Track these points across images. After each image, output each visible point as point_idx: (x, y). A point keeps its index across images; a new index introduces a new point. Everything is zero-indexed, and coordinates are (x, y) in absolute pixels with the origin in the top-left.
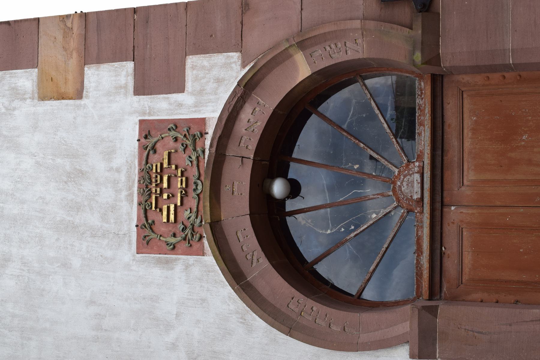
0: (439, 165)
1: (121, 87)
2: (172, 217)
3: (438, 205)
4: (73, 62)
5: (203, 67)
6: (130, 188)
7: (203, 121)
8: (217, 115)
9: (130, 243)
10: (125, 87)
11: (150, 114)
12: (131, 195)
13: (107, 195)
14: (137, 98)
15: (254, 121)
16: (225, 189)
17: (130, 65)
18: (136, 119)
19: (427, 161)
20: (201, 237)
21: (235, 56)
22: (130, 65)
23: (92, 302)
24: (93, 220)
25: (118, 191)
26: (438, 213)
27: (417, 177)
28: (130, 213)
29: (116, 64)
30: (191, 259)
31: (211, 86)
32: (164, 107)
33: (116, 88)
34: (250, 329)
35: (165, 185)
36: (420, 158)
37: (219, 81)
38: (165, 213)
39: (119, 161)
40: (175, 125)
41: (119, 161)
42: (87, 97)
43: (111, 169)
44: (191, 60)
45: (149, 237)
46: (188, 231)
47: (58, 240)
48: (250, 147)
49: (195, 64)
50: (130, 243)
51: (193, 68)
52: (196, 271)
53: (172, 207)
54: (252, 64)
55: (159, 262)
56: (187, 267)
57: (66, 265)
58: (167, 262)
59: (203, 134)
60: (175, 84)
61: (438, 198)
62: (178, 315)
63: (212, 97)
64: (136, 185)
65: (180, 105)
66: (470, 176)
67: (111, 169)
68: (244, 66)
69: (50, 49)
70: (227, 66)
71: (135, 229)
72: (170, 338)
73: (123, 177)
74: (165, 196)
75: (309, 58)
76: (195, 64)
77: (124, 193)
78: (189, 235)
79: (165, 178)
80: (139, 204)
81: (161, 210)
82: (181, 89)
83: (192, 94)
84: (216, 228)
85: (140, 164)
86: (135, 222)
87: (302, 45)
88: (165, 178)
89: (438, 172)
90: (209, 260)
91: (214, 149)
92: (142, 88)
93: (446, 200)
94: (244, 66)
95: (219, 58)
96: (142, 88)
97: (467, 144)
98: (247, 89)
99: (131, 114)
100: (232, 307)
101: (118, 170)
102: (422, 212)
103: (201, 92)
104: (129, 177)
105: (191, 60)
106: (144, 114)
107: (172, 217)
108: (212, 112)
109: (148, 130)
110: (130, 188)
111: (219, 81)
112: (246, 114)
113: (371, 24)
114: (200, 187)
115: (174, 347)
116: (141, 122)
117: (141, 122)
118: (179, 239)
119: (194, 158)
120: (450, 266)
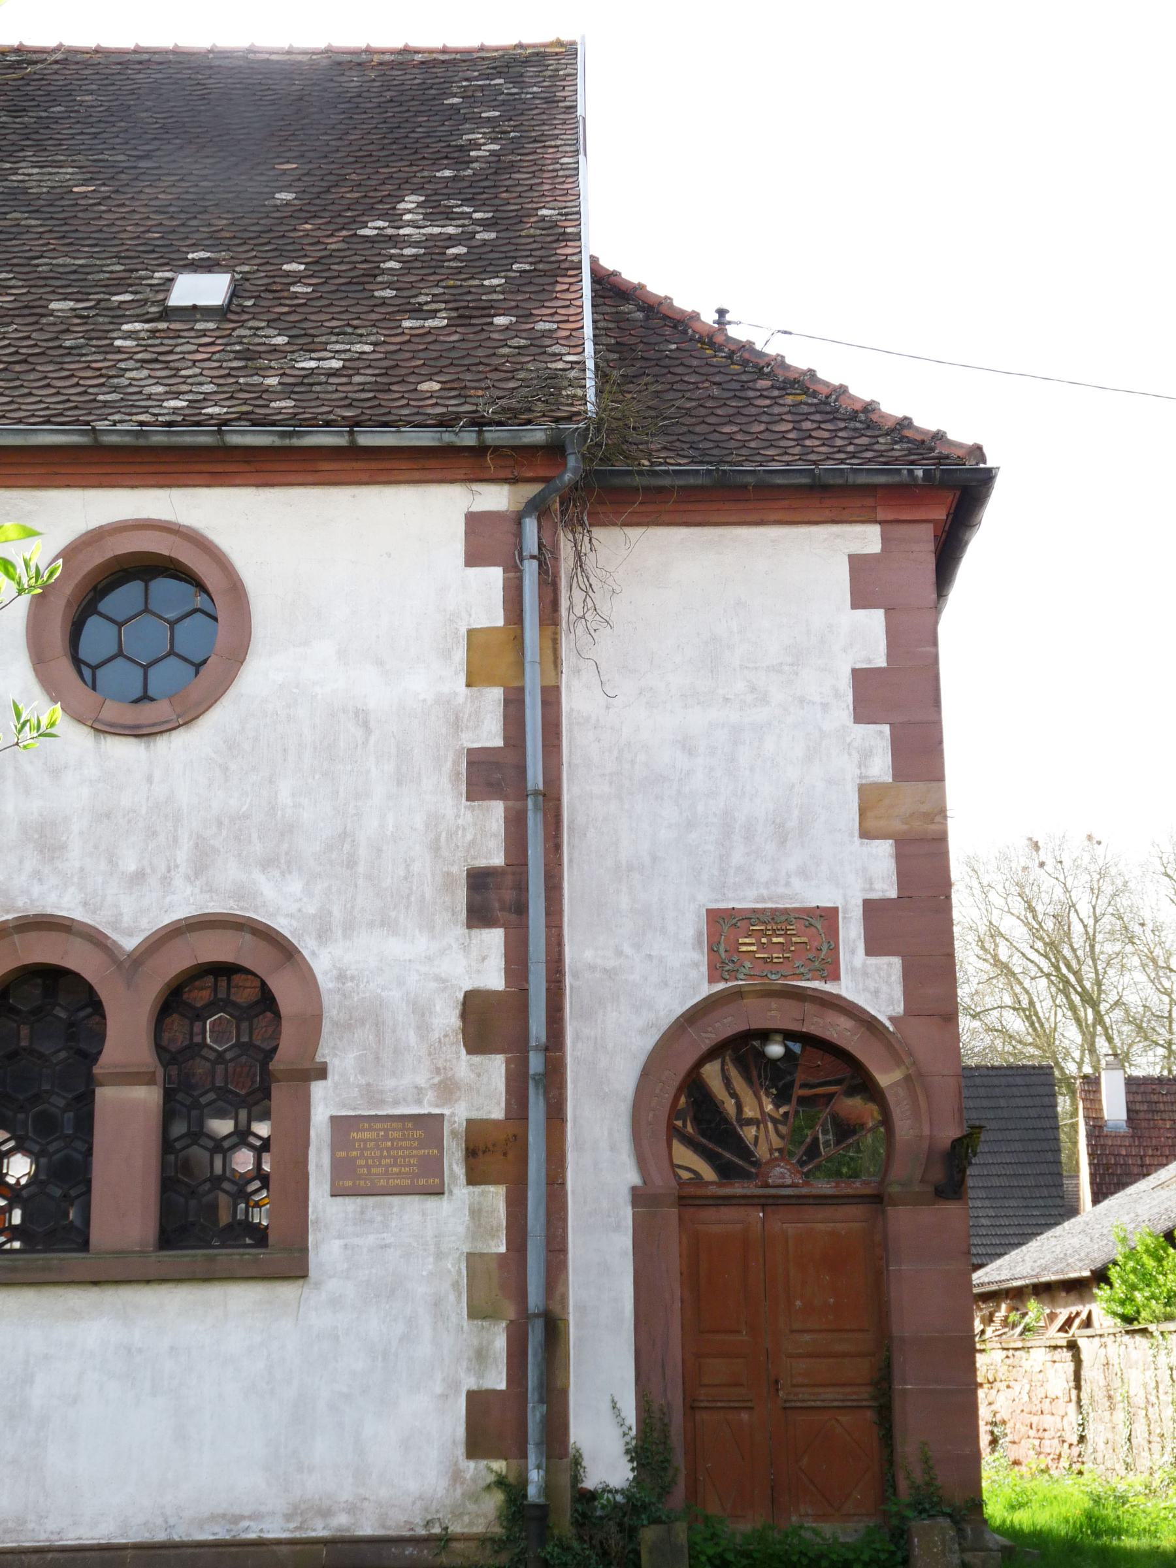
0: (801, 1201)
1: (871, 884)
2: (744, 948)
3: (763, 1201)
4: (898, 826)
5: (889, 976)
6: (770, 899)
7: (835, 976)
8: (844, 993)
9: (716, 901)
10: (872, 889)
11: (844, 918)
12: (763, 900)
13: (763, 872)
14: (860, 903)
15: (838, 1030)
16: (774, 1003)
17: (893, 894)
18: (839, 904)
19: (804, 1191)
20: (726, 980)
21: (899, 1009)
22: (893, 894)
23: (654, 859)
24: (738, 857)
25: (767, 885)
26: (756, 1201)
27: (789, 1181)
28: (745, 899)
29: (895, 878)
30: (704, 969)
31: (872, 985)
32: (851, 932)
33: (871, 879)
34: (642, 1032)
35: (775, 940)
36: (806, 1184)
37: (876, 993)
38: (747, 940)
39: (797, 884)
40: (835, 950)
41: (797, 884)
42: (862, 844)
43: (788, 876)
44: (896, 961)
45: (724, 927)
46: (730, 967)
47: (715, 814)
48: (812, 1027)
49: (891, 967)
50: (716, 901)
51: (890, 965)
52: (693, 974)
53: (754, 948)
54: (891, 1029)
55: (700, 934)
56: (696, 965)
57: (690, 825)
58: (700, 943)
59: (825, 979)
60: (874, 948)
61: (770, 1201)
62: (650, 956)
63: (861, 986)
64: (774, 906)
65: (853, 952)
66: (791, 1229)
67: (788, 876)
68: (891, 1019)
69: (912, 794)
70: (891, 1001)
71: (730, 907)
72: (627, 949)
73: (781, 890)
74: (764, 940)
75: (896, 1084)
76: (891, 967)
77: (765, 892)
78: (728, 968)
79: (781, 940)
80: (754, 911)
81: (749, 936)
82: (869, 952)
83: (864, 965)
84: (737, 994)
85: (795, 909)
86: (738, 906)
87: (908, 1078)
88: (781, 940)
89: (793, 1201)
90: (706, 989)
91: (810, 993)
92: (871, 908)
93: (769, 1209)
94: (891, 1019)
95: (898, 993)
96: (871, 908)
97: (820, 1226)
98: (869, 1023)
99: (845, 896)
100: (662, 1013)
101: (788, 884)
102: (756, 1186)
103: (865, 974)
104: (782, 897)
105: (896, 961)
106: (845, 912)
107: (744, 948)
108: (846, 988)
109: (828, 917)
110: (770, 899)
111: (876, 993)
112: (845, 1023)
113: (925, 1145)
114: (773, 977)
115: (619, 953)
116: (836, 909)
117: (836, 909)
118: (723, 955)
119: (802, 970)
120: (709, 1214)
